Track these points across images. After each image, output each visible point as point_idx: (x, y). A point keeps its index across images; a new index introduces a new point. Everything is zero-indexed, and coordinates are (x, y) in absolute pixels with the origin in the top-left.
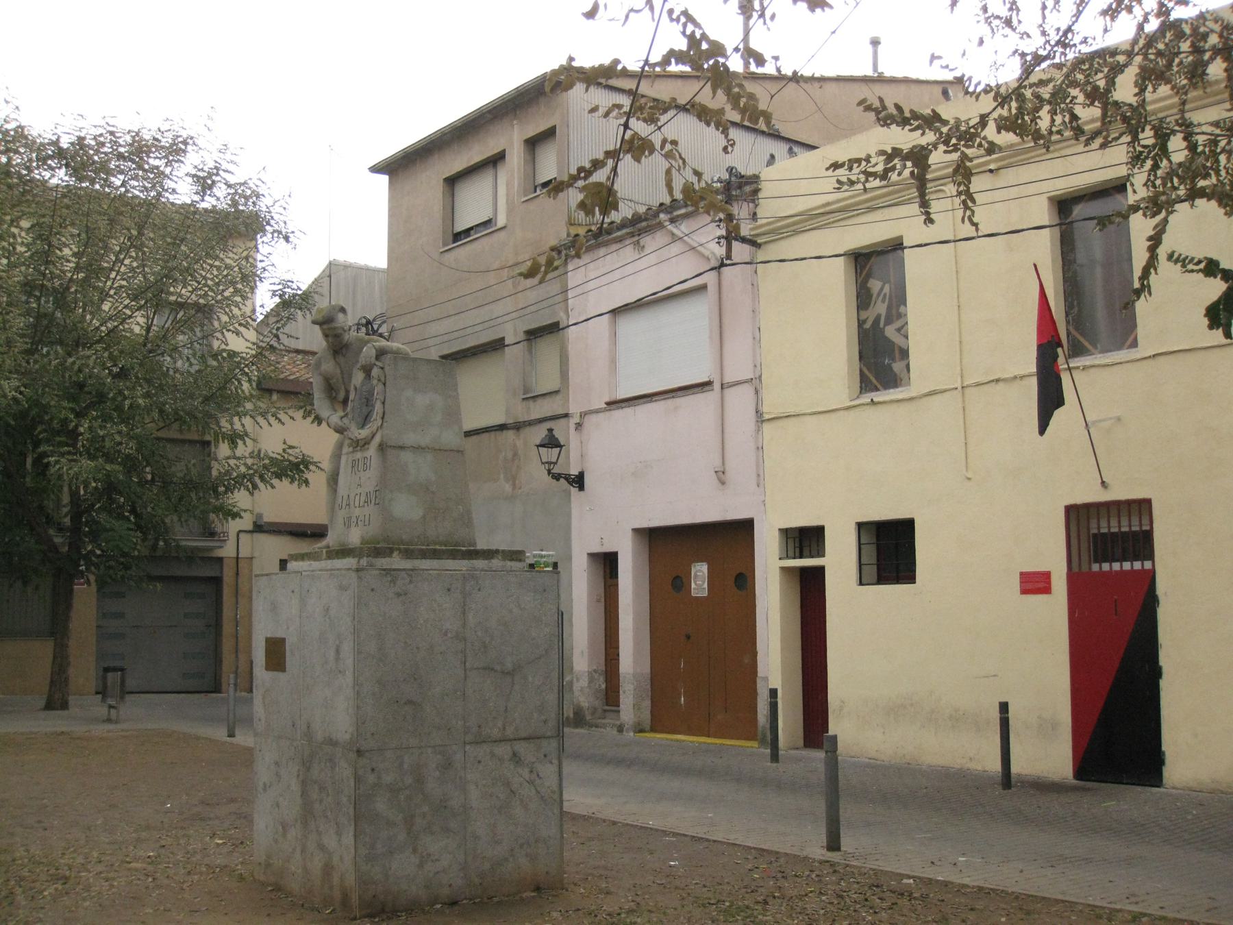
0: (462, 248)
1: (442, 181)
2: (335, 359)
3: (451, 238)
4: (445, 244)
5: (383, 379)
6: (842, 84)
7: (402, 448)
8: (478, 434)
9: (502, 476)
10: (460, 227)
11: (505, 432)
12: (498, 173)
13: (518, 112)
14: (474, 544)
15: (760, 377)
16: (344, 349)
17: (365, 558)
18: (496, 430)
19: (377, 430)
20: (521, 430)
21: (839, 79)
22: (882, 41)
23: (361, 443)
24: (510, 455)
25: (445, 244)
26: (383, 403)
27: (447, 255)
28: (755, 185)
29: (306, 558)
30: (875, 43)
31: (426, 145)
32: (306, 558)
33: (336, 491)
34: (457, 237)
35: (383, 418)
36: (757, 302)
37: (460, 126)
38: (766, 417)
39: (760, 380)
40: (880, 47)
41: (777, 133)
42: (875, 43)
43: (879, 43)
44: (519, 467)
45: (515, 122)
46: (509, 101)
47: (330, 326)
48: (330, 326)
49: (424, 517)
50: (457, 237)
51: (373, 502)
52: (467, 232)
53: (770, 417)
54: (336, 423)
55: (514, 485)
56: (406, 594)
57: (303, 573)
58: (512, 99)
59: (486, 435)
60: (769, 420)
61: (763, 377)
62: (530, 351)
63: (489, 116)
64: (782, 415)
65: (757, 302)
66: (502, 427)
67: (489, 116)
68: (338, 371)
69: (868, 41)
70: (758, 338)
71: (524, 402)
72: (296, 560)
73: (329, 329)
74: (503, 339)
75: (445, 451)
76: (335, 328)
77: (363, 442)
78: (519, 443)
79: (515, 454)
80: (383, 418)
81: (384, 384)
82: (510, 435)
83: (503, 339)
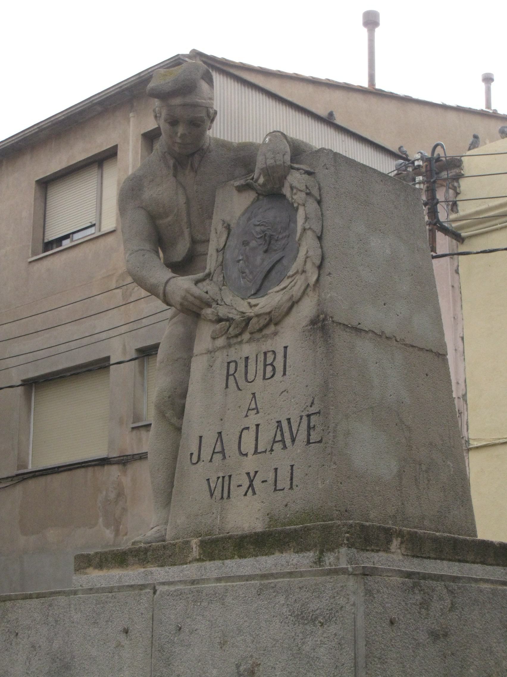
0: (57, 257)
1: (34, 183)
2: (175, 176)
3: (40, 247)
4: (34, 253)
5: (315, 192)
6: (461, 115)
7: (357, 330)
8: (70, 470)
9: (101, 520)
10: (51, 236)
11: (106, 467)
12: (105, 176)
13: (135, 104)
14: (476, 536)
15: (464, 396)
16: (197, 157)
17: (343, 550)
18: (96, 465)
19: (304, 293)
20: (129, 466)
21: (458, 109)
22: (495, 78)
23: (254, 324)
24: (112, 496)
25: (34, 253)
26: (320, 238)
27: (37, 266)
28: (457, 170)
29: (131, 559)
30: (488, 79)
31: (17, 143)
32: (131, 559)
33: (179, 429)
34: (48, 245)
35: (320, 267)
36: (459, 308)
37: (64, 120)
38: (475, 444)
39: (465, 401)
40: (493, 85)
41: (404, 156)
42: (488, 79)
43: (492, 80)
44: (124, 510)
45: (131, 115)
46: (126, 89)
47: (188, 100)
48: (188, 100)
49: (400, 475)
50: (48, 245)
51: (302, 436)
52: (59, 241)
53: (479, 445)
54: (187, 291)
55: (117, 532)
56: (446, 635)
57: (160, 589)
58: (131, 87)
59: (80, 472)
60: (477, 448)
61: (469, 395)
62: (142, 373)
63: (99, 109)
64: (497, 442)
65: (459, 308)
66: (103, 462)
67: (99, 109)
68: (182, 199)
69: (480, 78)
70: (461, 349)
71: (134, 432)
72: (100, 566)
73: (184, 105)
74: (108, 358)
75: (421, 349)
76: (194, 106)
77: (263, 322)
78: (126, 481)
79: (120, 494)
80: (320, 267)
81: (319, 202)
82: (114, 471)
83: (108, 358)
